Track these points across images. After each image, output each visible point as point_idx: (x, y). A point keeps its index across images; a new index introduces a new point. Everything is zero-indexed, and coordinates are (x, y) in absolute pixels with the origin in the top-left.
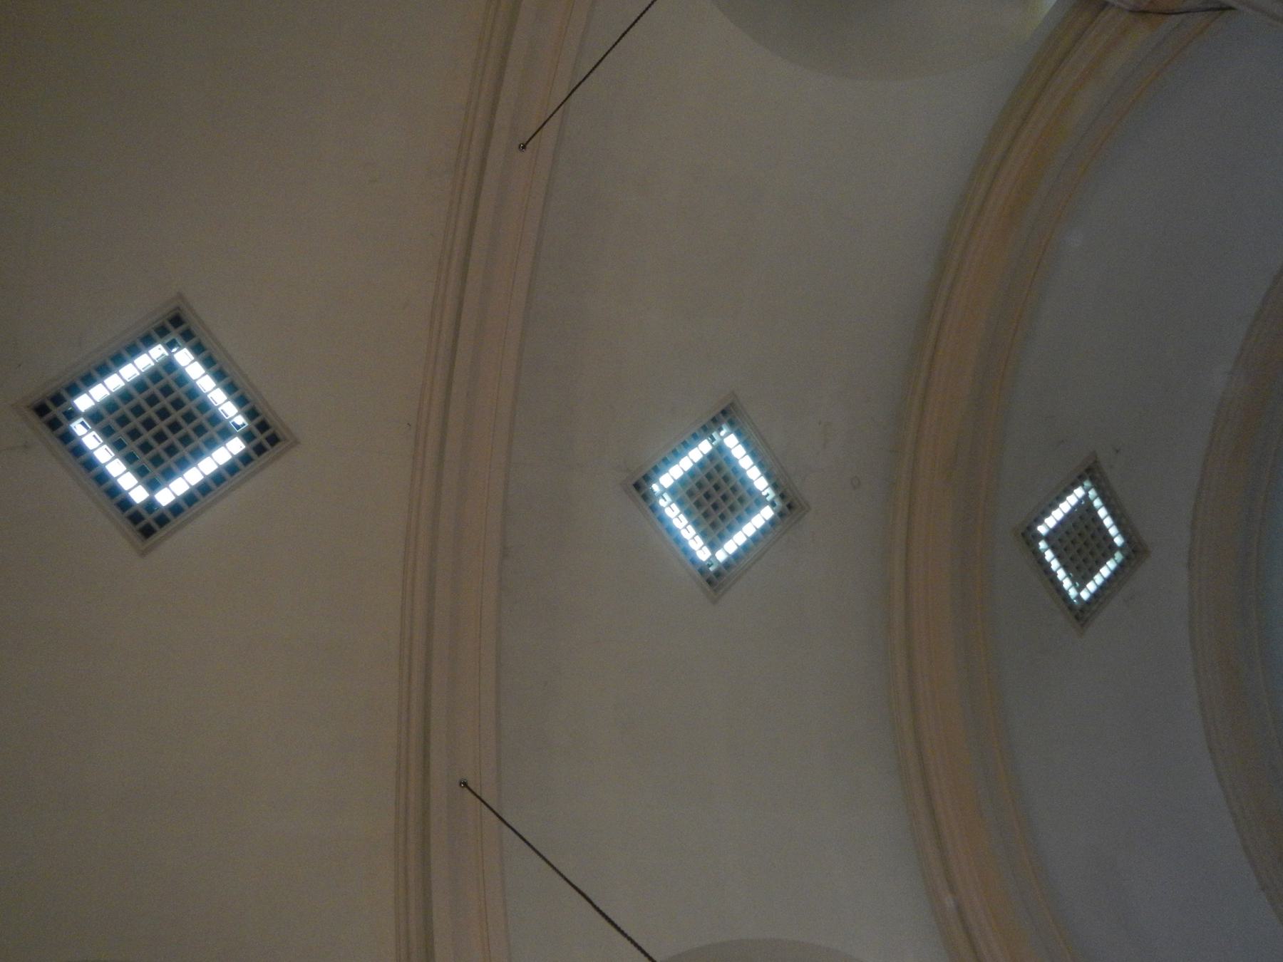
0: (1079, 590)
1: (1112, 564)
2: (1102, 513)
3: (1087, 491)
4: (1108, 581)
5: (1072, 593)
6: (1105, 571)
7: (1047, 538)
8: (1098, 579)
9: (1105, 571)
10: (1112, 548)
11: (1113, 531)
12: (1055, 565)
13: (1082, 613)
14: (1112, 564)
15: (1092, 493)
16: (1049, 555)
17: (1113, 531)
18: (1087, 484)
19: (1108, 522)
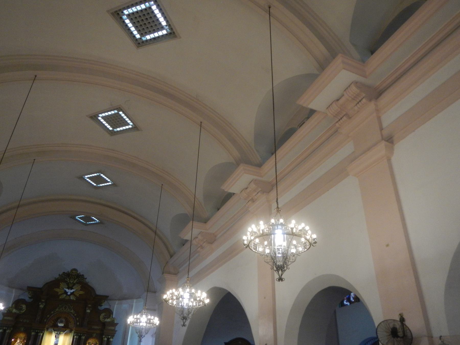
0: (78, 217)
1: (83, 221)
2: (94, 222)
4: (80, 221)
5: (77, 217)
6: (82, 221)
8: (80, 220)
9: (82, 221)
10: (86, 222)
11: (90, 223)
13: (73, 217)
14: (83, 221)
15: (98, 222)
17: (90, 223)
18: (99, 222)
19: (92, 222)
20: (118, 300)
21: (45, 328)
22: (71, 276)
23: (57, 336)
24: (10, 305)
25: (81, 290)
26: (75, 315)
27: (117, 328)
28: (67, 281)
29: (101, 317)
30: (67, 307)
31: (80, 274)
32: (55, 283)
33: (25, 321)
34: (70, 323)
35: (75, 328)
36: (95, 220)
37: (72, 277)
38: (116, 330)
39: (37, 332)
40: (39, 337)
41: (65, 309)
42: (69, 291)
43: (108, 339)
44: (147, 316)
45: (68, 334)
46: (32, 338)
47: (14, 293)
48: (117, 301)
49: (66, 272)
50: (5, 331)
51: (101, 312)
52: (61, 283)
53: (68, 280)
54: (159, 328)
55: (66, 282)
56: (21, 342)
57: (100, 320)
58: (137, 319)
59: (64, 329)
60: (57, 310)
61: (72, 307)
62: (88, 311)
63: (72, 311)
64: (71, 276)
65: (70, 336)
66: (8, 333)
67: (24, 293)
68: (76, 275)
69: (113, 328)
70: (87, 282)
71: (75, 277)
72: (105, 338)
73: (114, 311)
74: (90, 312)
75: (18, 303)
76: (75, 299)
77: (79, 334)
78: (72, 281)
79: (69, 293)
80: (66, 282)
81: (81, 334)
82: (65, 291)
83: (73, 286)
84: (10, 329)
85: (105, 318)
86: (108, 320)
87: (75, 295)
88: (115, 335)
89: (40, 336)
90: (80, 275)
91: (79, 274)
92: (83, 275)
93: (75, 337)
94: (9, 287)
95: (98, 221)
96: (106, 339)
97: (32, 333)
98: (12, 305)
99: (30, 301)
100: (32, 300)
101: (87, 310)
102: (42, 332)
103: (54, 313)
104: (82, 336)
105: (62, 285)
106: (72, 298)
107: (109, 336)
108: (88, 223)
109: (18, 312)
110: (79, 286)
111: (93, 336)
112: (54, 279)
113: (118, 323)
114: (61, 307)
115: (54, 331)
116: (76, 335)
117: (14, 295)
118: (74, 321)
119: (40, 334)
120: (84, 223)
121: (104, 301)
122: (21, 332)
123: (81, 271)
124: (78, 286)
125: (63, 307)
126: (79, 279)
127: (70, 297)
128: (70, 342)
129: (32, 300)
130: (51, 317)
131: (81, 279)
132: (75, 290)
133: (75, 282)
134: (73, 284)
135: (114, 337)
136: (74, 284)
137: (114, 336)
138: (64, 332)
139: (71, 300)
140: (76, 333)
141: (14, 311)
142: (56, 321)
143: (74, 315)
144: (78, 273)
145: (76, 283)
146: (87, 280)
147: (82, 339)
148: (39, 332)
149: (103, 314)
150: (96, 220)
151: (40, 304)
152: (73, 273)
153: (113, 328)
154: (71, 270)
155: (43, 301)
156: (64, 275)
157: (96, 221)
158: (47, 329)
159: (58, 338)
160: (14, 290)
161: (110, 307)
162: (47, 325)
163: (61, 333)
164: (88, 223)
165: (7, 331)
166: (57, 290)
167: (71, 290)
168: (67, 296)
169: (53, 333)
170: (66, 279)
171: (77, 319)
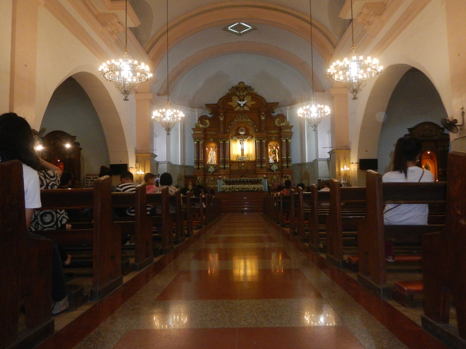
1: (236, 32)
2: (247, 30)
3: (251, 28)
4: (233, 31)
5: (229, 27)
6: (235, 31)
7: (239, 24)
8: (233, 30)
9: (235, 31)
10: (240, 31)
11: (243, 31)
12: (234, 25)
13: (226, 29)
14: (236, 32)
15: (250, 29)
16: (236, 24)
17: (243, 31)
18: (252, 28)
19: (245, 31)
20: (289, 105)
21: (229, 137)
22: (240, 90)
23: (241, 143)
24: (197, 122)
25: (252, 101)
26: (252, 123)
27: (293, 130)
28: (237, 95)
29: (276, 123)
30: (244, 117)
31: (247, 86)
32: (227, 98)
33: (212, 133)
34: (250, 130)
35: (254, 133)
36: (247, 27)
37: (241, 90)
38: (292, 131)
39: (224, 140)
40: (227, 145)
41: (242, 119)
42: (242, 103)
43: (287, 140)
44: (316, 105)
45: (250, 140)
46: (221, 146)
47: (196, 111)
48: (288, 106)
49: (234, 86)
50: (198, 142)
51: (274, 118)
52: (232, 97)
53: (238, 93)
54: (333, 117)
55: (236, 95)
56: (214, 150)
57: (275, 126)
58: (307, 110)
59: (246, 136)
60: (236, 120)
61: (248, 116)
62: (263, 118)
63: (249, 120)
64: (240, 88)
65: (253, 141)
66: (201, 144)
67: (205, 111)
68: (243, 87)
69: (289, 130)
70: (256, 92)
71: (243, 90)
72: (283, 139)
73: (287, 116)
74: (265, 118)
75: (202, 119)
76: (248, 110)
77: (260, 139)
78: (242, 93)
79: (242, 105)
80: (236, 95)
81: (261, 138)
82: (238, 103)
83: (244, 98)
84: (202, 141)
85: (279, 123)
86: (284, 124)
87: (247, 106)
88: (292, 136)
89: (227, 143)
90: (248, 87)
91: (246, 86)
92: (250, 87)
93: (257, 141)
94: (191, 107)
95: (250, 27)
96: (284, 141)
97: (220, 142)
98: (198, 121)
99: (212, 116)
100: (212, 115)
101: (262, 118)
102: (228, 141)
103: (234, 123)
104: (263, 140)
105: (235, 99)
106: (246, 108)
107: (287, 138)
108: (241, 32)
109: (204, 127)
110: (249, 98)
111: (272, 139)
112: (225, 94)
113: (292, 125)
114: (238, 118)
115: (238, 139)
116: (257, 140)
117: (197, 113)
118: (253, 129)
119: (227, 142)
120: (238, 33)
121: (276, 108)
122: (211, 142)
123: (247, 83)
124: (248, 98)
125: (240, 117)
126: (247, 90)
127: (243, 108)
128: (253, 146)
129: (212, 115)
130: (232, 126)
131: (249, 91)
132: (247, 101)
133: (245, 94)
134: (243, 96)
135: (291, 138)
136: (244, 97)
137: (291, 137)
138: (247, 138)
139: (245, 110)
140: (257, 138)
141: (201, 126)
142: (238, 129)
143: (251, 123)
144: (245, 85)
145: (245, 95)
146: (255, 91)
147: (263, 142)
148: (226, 141)
149: (277, 120)
150: (248, 26)
151: (220, 118)
152: (240, 86)
153: (289, 130)
154: (239, 84)
155: (222, 114)
156: (233, 89)
157: (248, 28)
158: (232, 138)
159: (243, 144)
160: (196, 110)
161: (283, 113)
162: (230, 135)
163: (244, 139)
164: (241, 32)
165: (201, 143)
166: (230, 103)
167: (243, 101)
168: (241, 108)
169: (238, 140)
170: (237, 93)
171: (255, 126)
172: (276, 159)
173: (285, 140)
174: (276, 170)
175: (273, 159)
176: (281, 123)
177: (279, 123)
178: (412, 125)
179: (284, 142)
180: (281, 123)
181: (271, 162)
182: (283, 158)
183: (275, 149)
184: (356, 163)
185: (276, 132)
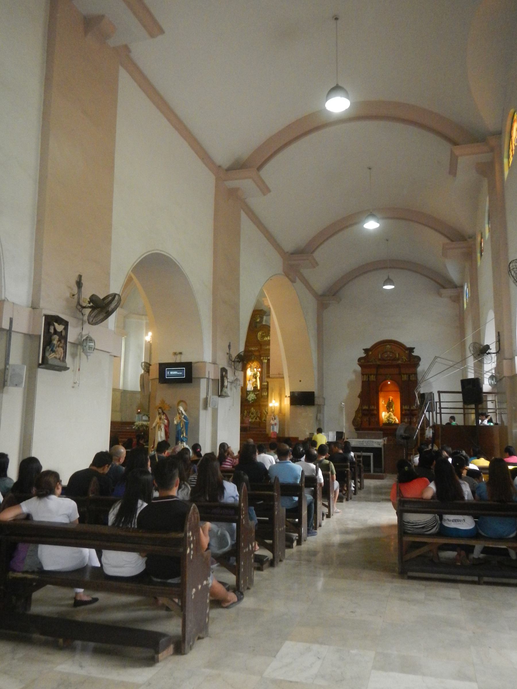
72: (263, 359)
85: (263, 337)
96: (266, 361)
172: (257, 386)
173: (266, 360)
174: (252, 400)
175: (253, 386)
176: (265, 337)
177: (263, 337)
178: (368, 346)
179: (264, 363)
180: (265, 337)
181: (248, 390)
182: (263, 384)
183: (256, 371)
184: (289, 397)
185: (257, 349)
